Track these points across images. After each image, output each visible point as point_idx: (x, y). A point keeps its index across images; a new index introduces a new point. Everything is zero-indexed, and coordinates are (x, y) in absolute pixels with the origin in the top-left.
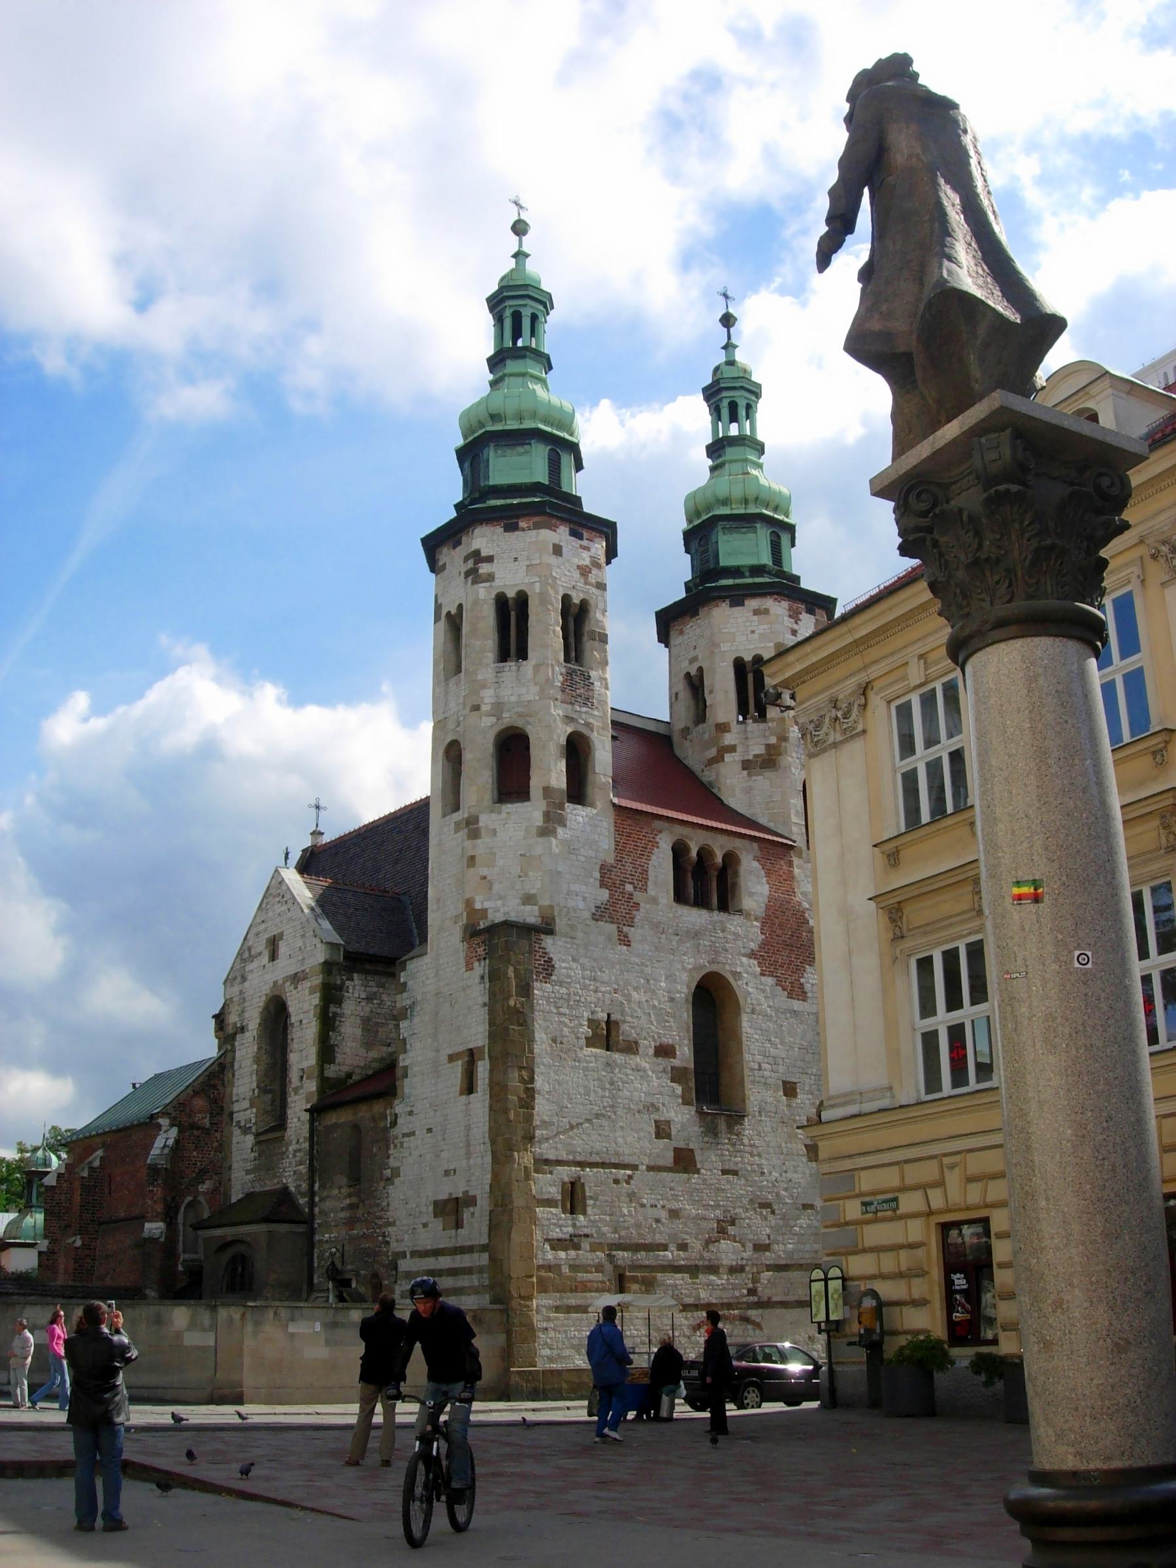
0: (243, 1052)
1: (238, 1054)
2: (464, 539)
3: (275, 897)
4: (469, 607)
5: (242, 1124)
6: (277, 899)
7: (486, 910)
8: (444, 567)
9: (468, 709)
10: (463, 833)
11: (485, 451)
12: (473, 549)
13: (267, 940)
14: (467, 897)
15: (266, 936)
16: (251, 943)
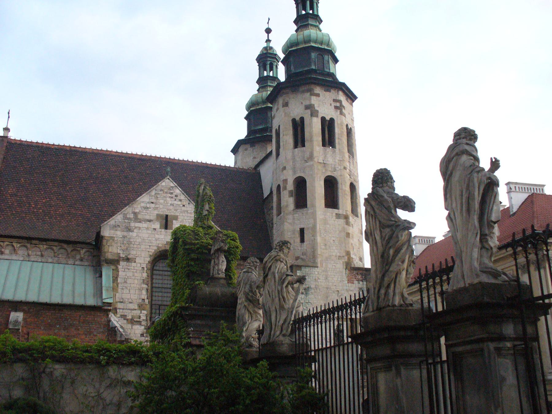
0: (130, 274)
1: (120, 273)
2: (332, 91)
3: (166, 193)
4: (339, 122)
5: (129, 317)
6: (170, 195)
7: (353, 258)
8: (318, 95)
9: (342, 167)
10: (342, 221)
11: (326, 57)
12: (339, 99)
13: (157, 214)
14: (348, 250)
15: (157, 213)
16: (137, 211)
